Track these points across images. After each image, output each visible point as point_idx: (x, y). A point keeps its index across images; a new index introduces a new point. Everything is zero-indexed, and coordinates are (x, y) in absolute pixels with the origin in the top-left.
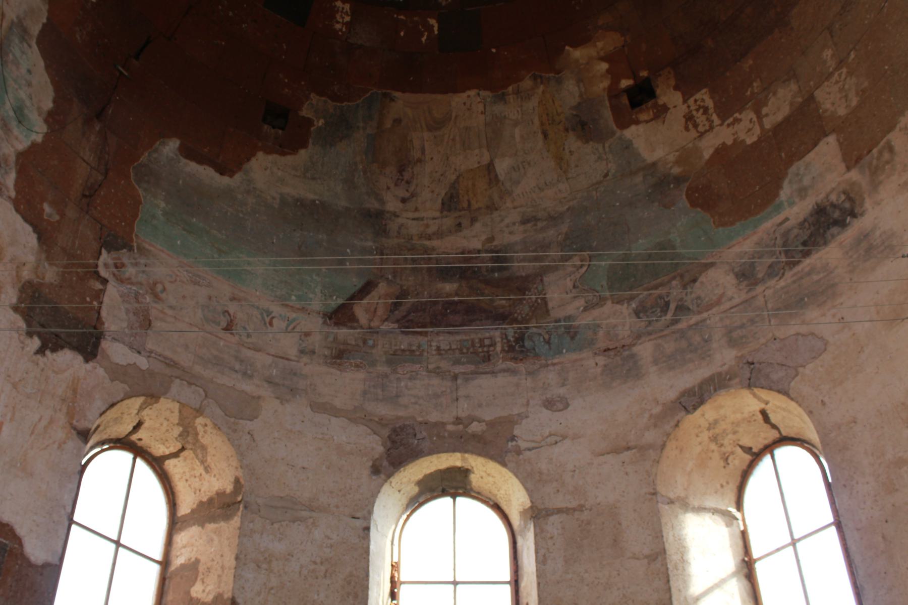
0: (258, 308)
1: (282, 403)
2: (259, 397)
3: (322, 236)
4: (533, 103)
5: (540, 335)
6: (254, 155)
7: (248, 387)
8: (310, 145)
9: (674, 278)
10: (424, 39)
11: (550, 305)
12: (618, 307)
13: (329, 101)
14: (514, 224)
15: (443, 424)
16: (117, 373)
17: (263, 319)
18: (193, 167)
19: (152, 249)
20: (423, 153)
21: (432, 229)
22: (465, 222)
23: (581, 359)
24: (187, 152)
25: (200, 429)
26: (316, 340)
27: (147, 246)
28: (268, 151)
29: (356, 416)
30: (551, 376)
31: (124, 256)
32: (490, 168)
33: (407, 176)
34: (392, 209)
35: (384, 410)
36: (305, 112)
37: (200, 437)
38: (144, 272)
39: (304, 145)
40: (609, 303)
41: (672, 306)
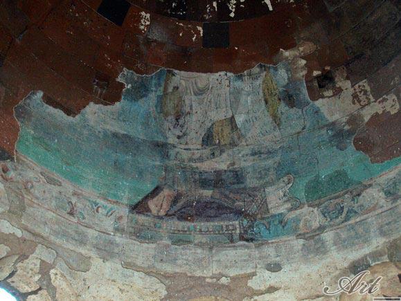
0: (89, 201)
1: (104, 262)
2: (90, 257)
3: (129, 157)
4: (259, 82)
5: (264, 224)
6: (88, 104)
7: (83, 251)
8: (122, 101)
9: (346, 193)
10: (194, 39)
11: (270, 206)
12: (311, 209)
13: (134, 73)
14: (247, 155)
15: (205, 278)
17: (92, 207)
18: (51, 109)
19: (25, 160)
20: (191, 109)
21: (197, 156)
22: (217, 153)
23: (289, 240)
24: (49, 100)
25: (53, 277)
26: (125, 221)
27: (22, 158)
28: (96, 103)
30: (269, 251)
31: (9, 164)
32: (232, 119)
33: (181, 122)
34: (172, 143)
35: (169, 268)
36: (120, 79)
37: (52, 281)
38: (20, 175)
39: (118, 99)
40: (306, 206)
41: (345, 210)
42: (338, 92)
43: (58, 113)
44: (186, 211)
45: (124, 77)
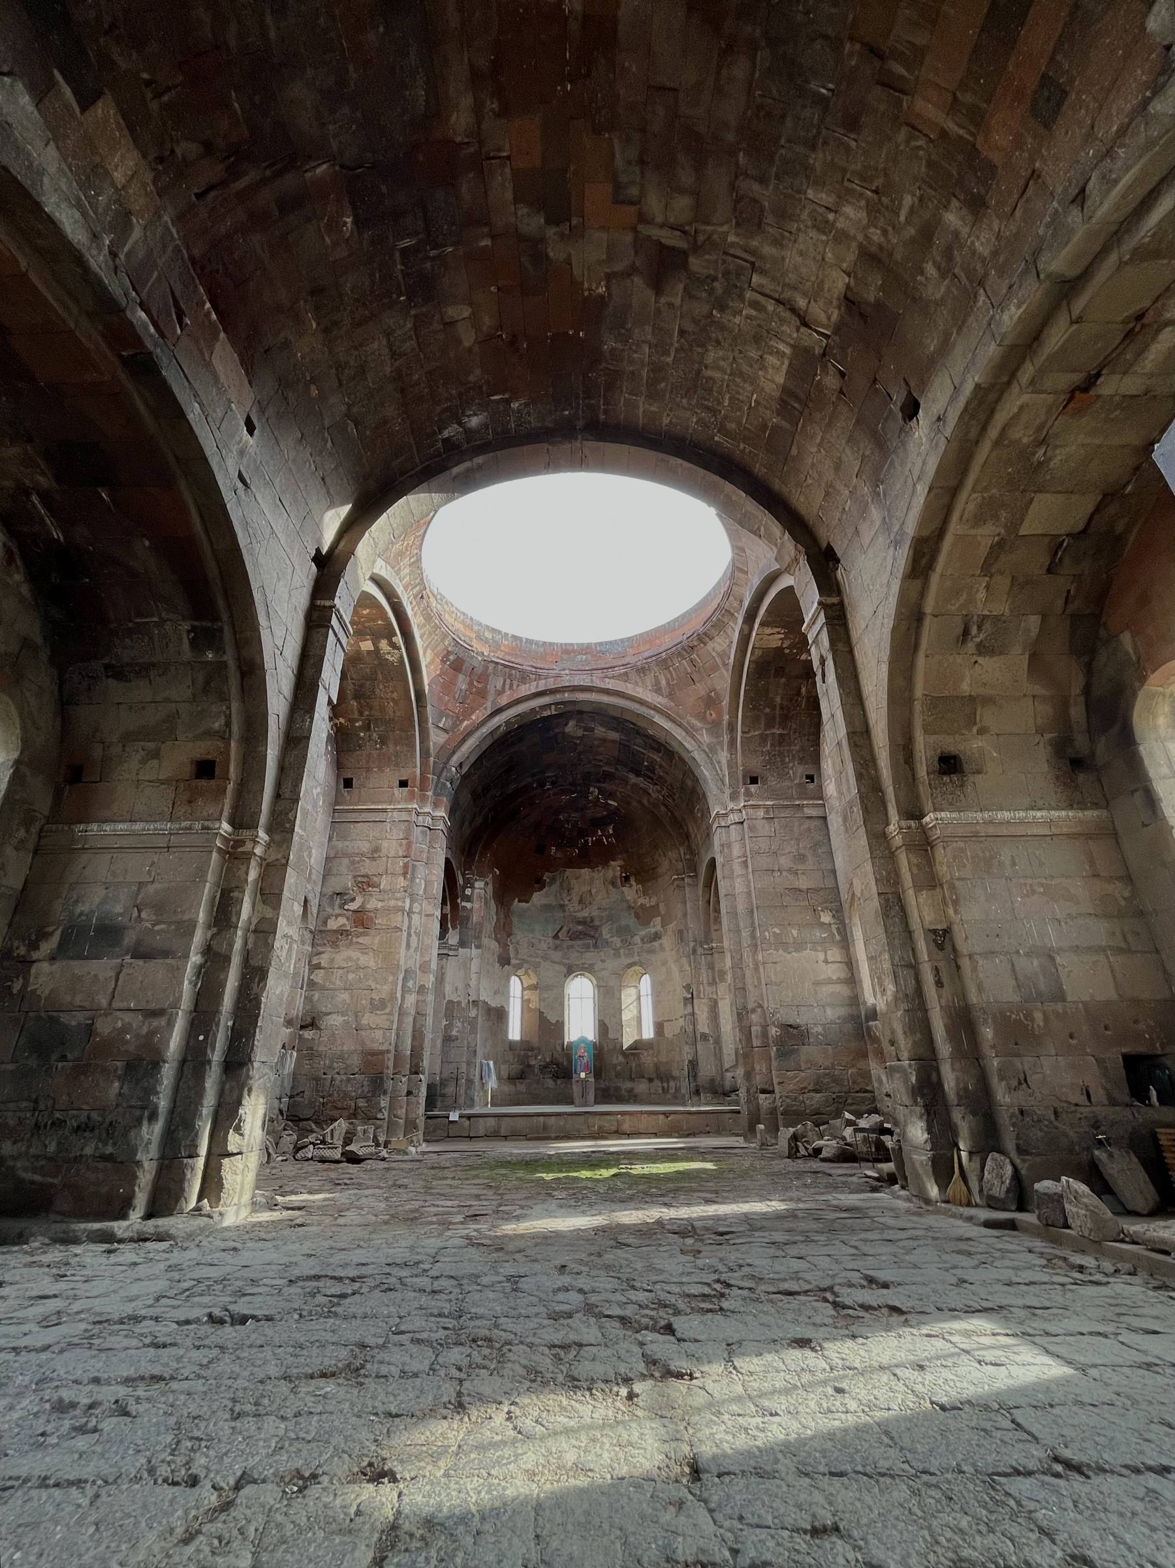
16: (514, 966)
29: (560, 963)
42: (631, 886)
43: (524, 904)
44: (574, 936)
45: (546, 877)
